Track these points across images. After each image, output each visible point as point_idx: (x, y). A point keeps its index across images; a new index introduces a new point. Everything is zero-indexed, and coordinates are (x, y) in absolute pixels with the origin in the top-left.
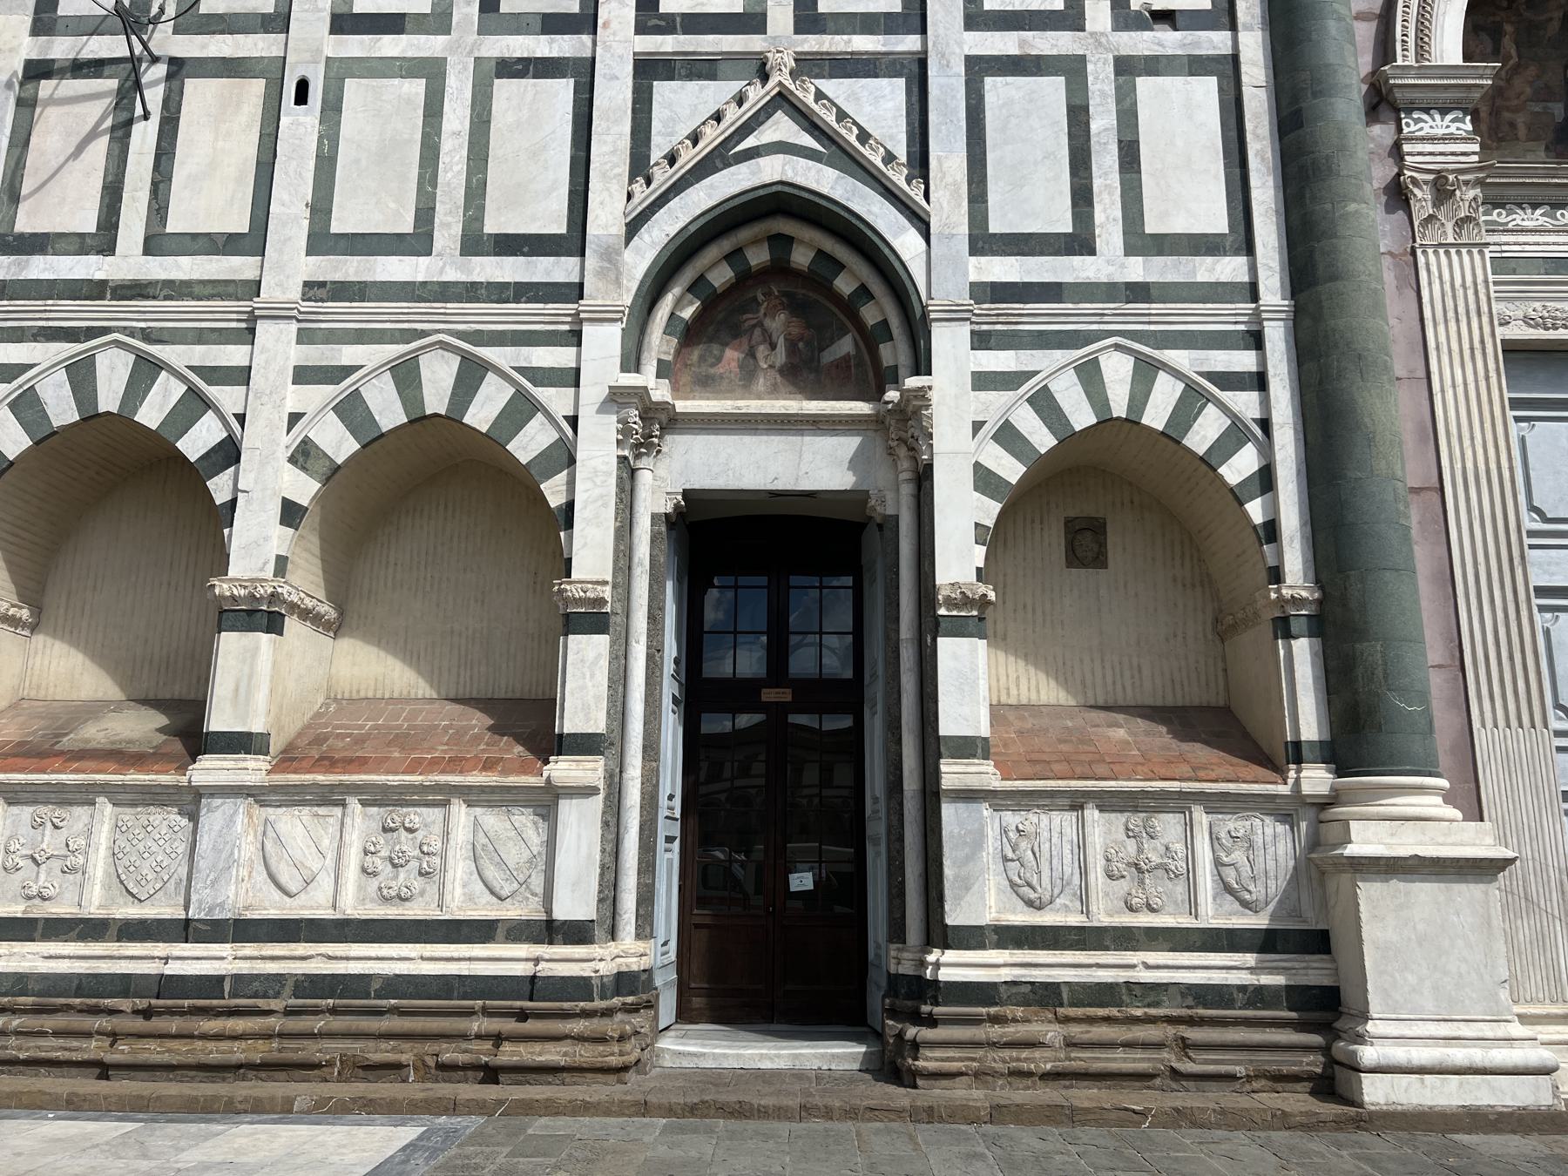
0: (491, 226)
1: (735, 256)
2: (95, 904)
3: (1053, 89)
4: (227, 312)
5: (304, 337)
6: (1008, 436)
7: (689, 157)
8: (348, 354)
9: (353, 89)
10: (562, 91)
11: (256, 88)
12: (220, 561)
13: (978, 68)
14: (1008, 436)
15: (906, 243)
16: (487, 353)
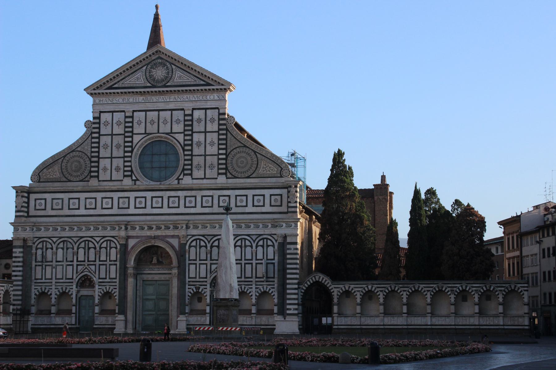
0: (68, 277)
1: (84, 278)
2: (46, 323)
3: (105, 266)
4: (50, 284)
5: (55, 286)
6: (101, 292)
7: (80, 272)
8: (58, 287)
9: (58, 267)
10: (71, 267)
11: (51, 267)
12: (51, 302)
13: (100, 265)
14: (101, 292)
15: (94, 279)
16: (68, 287)
